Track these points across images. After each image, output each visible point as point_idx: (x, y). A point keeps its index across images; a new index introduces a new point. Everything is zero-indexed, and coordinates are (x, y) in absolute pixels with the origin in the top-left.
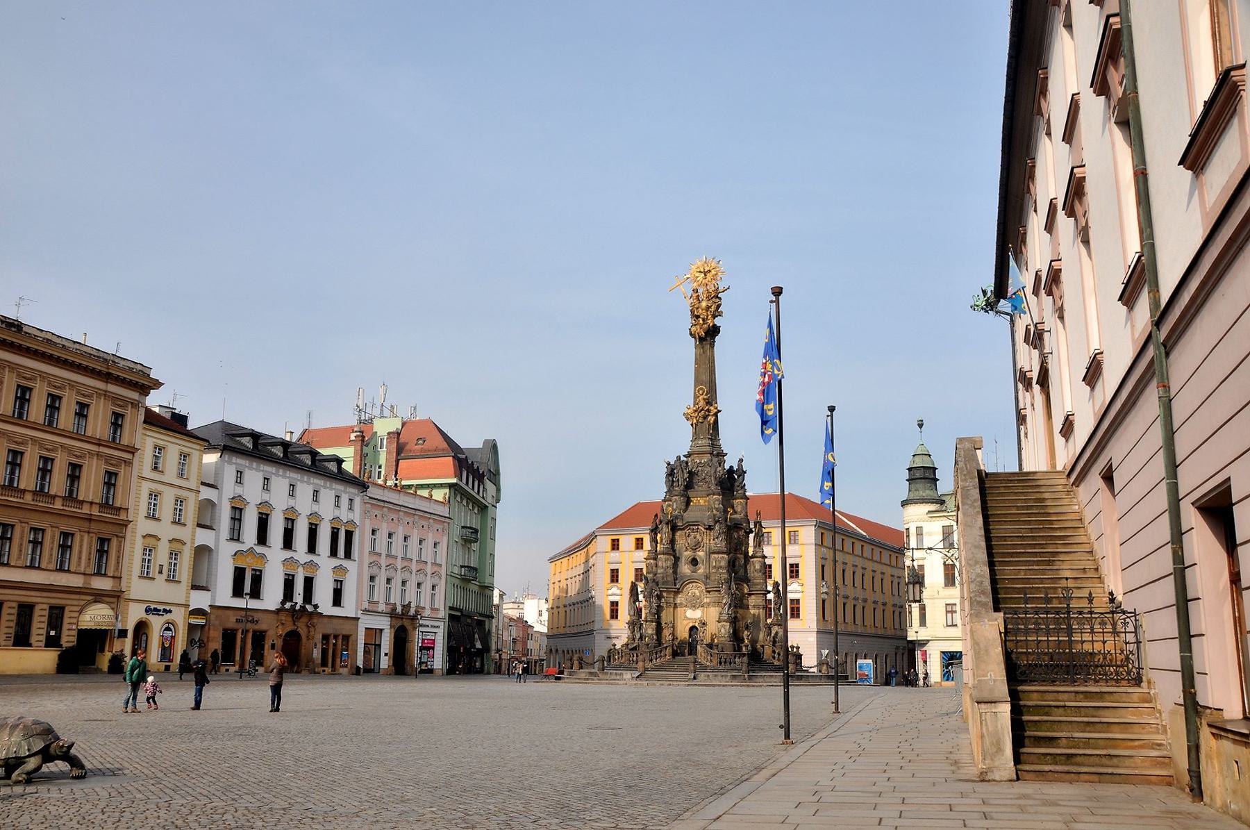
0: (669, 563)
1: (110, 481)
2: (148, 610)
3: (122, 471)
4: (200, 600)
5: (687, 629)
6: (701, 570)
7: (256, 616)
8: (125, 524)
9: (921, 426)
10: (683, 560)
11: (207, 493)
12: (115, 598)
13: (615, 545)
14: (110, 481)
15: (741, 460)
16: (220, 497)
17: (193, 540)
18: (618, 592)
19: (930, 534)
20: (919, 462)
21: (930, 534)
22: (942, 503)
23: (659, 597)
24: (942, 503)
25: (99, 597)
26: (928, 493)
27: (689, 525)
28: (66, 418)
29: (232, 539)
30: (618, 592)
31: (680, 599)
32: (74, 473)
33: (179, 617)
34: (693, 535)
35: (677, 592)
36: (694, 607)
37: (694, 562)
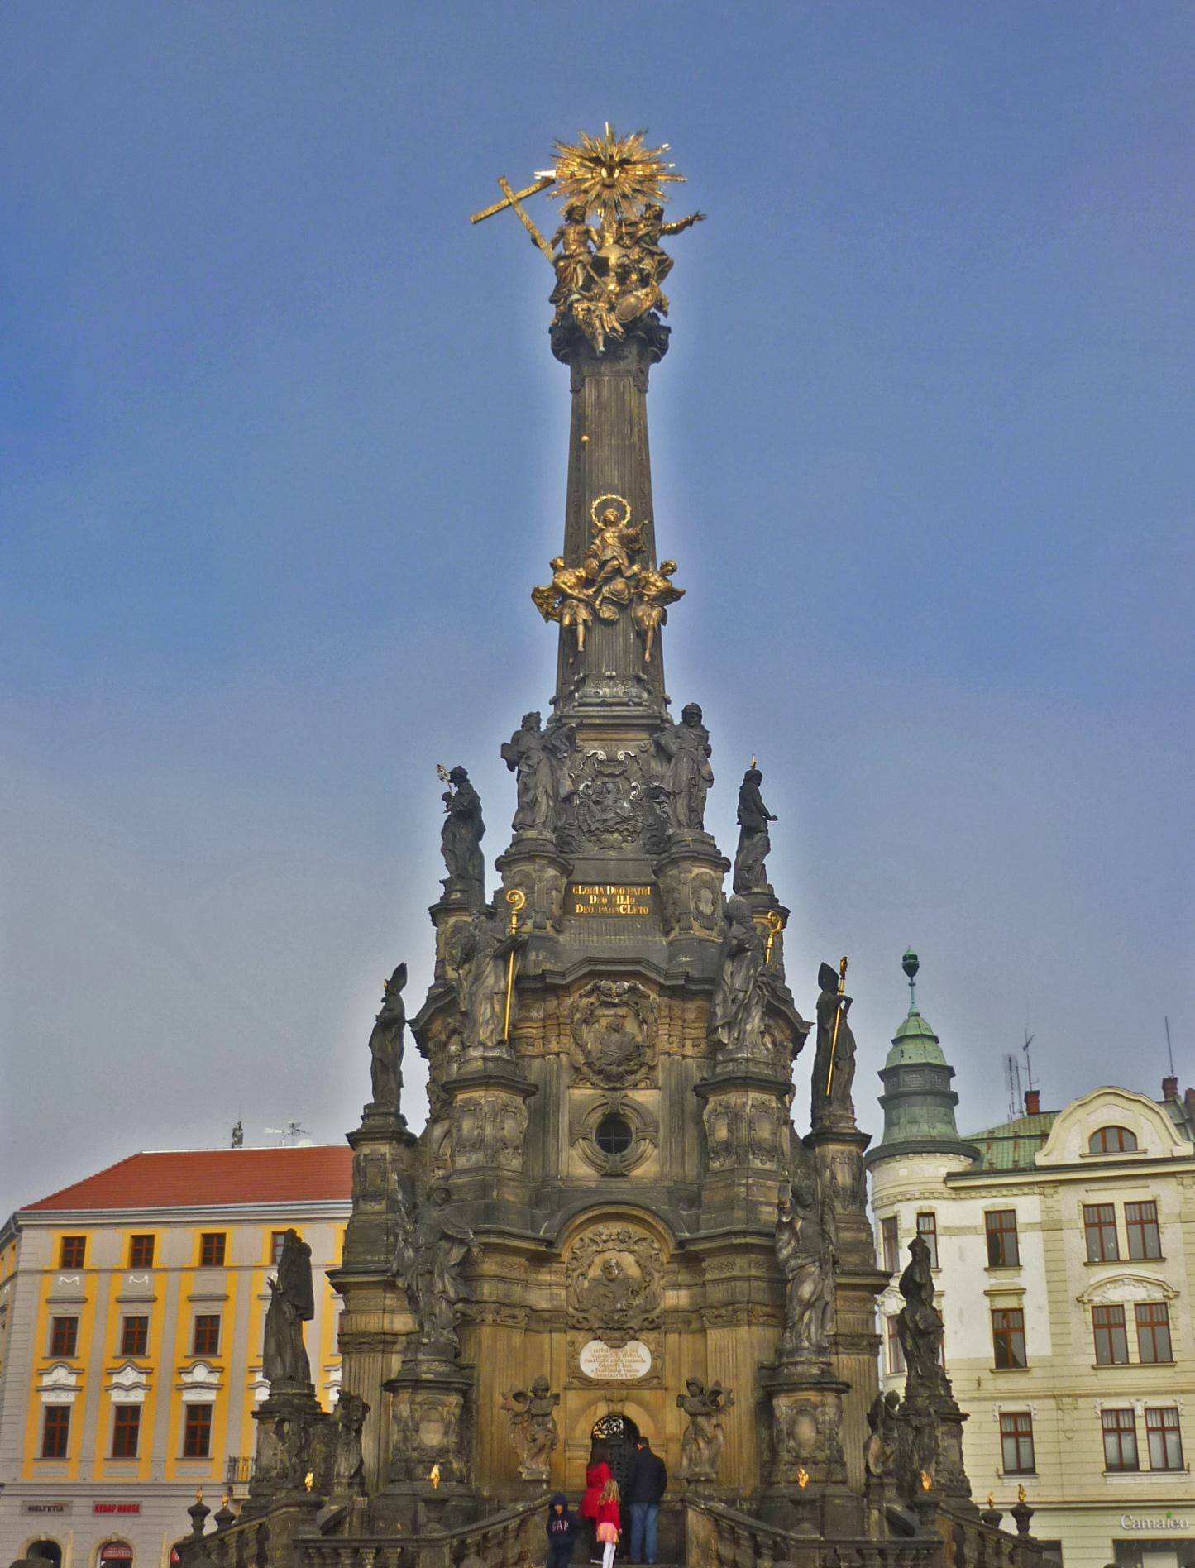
0: (511, 1128)
5: (582, 1433)
6: (648, 1165)
9: (911, 966)
10: (564, 1121)
13: (73, 1254)
15: (753, 778)
18: (72, 1380)
19: (953, 1231)
20: (914, 1054)
21: (953, 1231)
22: (975, 1156)
23: (466, 1272)
24: (975, 1156)
26: (939, 1130)
27: (596, 971)
30: (72, 1380)
31: (546, 1291)
34: (606, 1017)
35: (542, 1258)
36: (616, 1332)
37: (614, 1133)
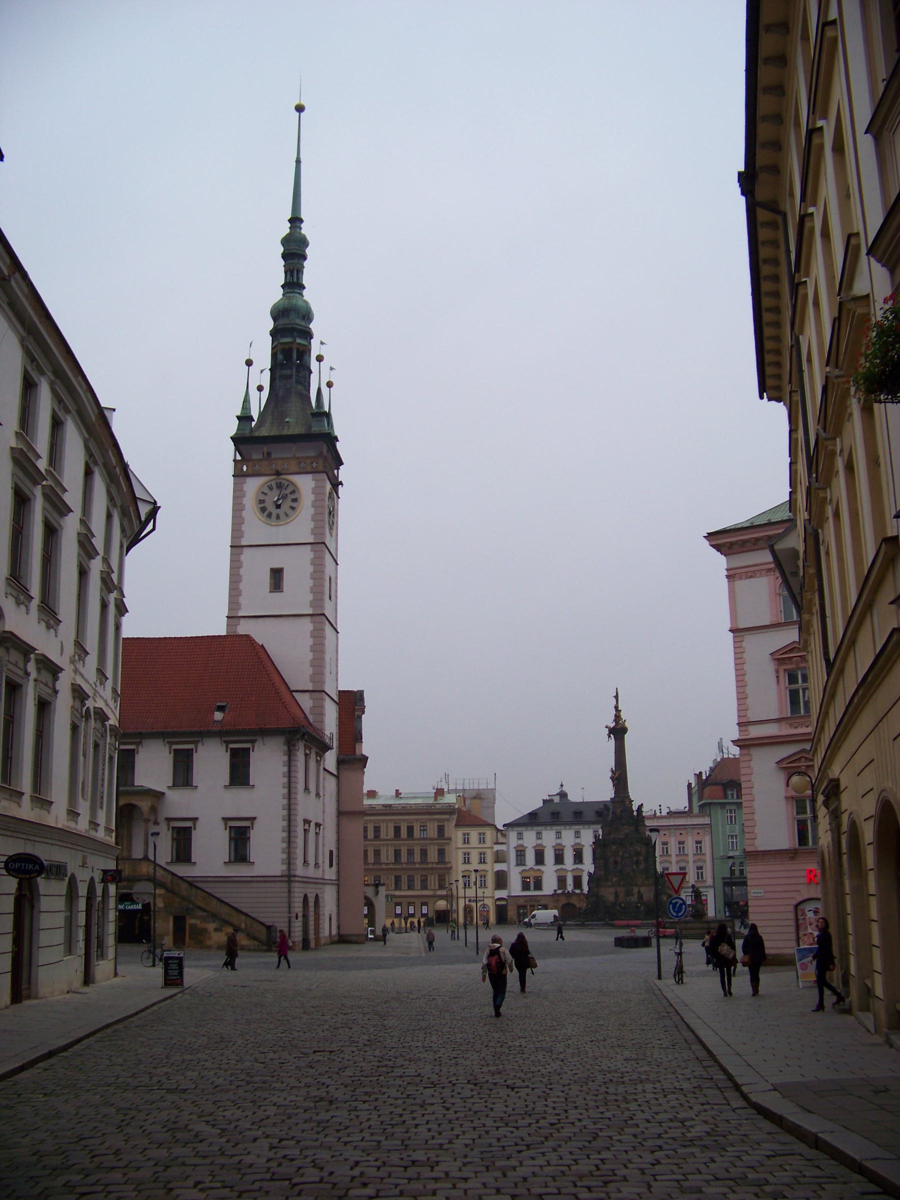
1: (441, 852)
2: (470, 901)
3: (447, 848)
4: (503, 894)
7: (538, 898)
8: (451, 868)
11: (497, 847)
12: (449, 898)
14: (441, 852)
16: (508, 848)
17: (493, 869)
25: (441, 897)
28: (417, 833)
29: (517, 865)
32: (424, 853)
33: (489, 902)
